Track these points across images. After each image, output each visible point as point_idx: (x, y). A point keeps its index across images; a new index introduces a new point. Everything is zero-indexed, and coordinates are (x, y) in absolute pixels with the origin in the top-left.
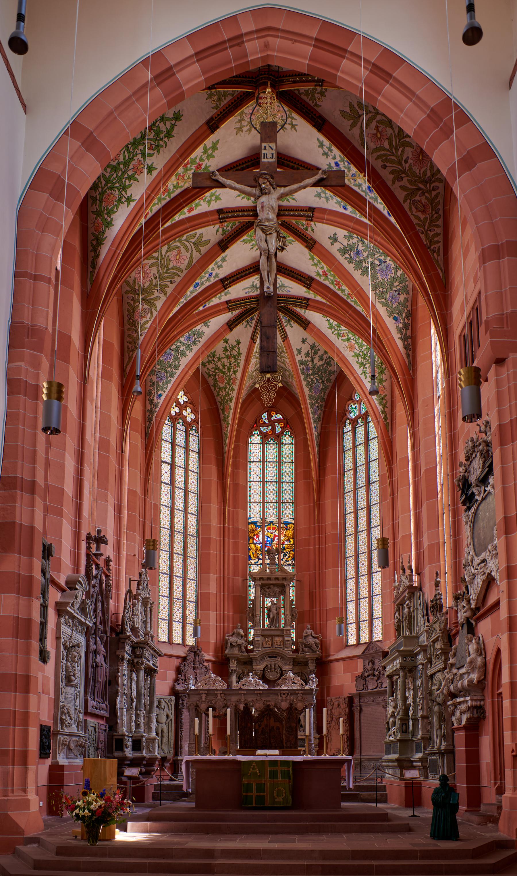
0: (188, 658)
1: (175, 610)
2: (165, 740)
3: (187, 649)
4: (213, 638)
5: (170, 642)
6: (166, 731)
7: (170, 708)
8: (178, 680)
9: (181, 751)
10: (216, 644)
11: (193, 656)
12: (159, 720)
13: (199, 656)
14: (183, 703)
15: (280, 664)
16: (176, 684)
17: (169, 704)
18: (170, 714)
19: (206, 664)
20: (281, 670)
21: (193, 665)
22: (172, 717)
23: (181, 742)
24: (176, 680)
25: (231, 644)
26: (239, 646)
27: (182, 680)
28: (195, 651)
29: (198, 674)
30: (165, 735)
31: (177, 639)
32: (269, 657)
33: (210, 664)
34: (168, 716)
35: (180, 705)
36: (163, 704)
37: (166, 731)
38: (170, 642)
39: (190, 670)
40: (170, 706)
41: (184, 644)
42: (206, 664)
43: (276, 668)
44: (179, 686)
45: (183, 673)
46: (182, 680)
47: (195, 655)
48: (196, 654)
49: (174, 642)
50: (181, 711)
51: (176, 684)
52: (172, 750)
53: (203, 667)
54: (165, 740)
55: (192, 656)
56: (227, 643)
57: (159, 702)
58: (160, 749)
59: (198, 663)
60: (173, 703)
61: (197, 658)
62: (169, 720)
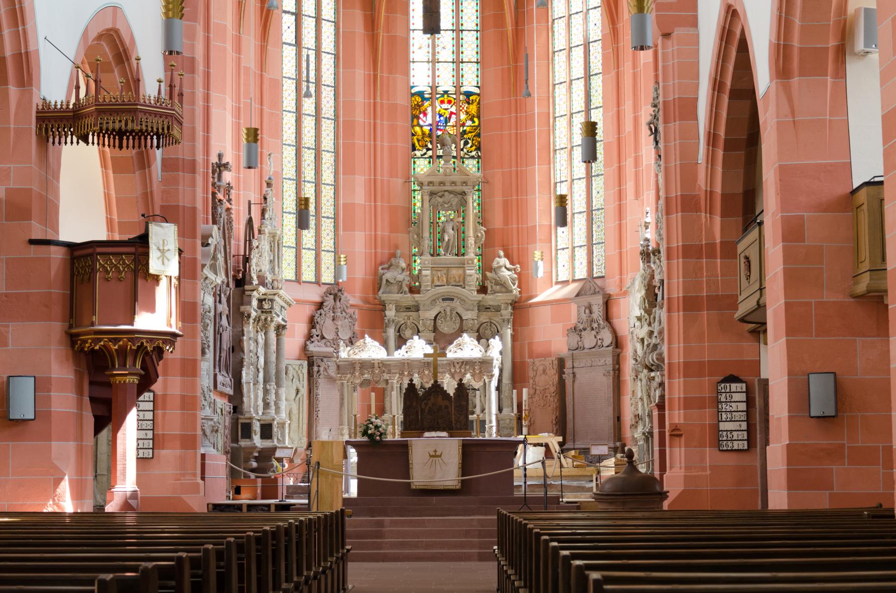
0: (325, 304)
3: (324, 288)
5: (298, 280)
6: (295, 411)
7: (301, 379)
8: (312, 337)
13: (340, 300)
14: (318, 371)
16: (308, 343)
17: (299, 372)
18: (301, 388)
19: (351, 311)
20: (461, 317)
21: (333, 314)
22: (304, 391)
23: (316, 427)
24: (309, 337)
25: (387, 281)
26: (400, 284)
27: (317, 336)
28: (335, 292)
29: (339, 327)
31: (308, 275)
32: (443, 300)
33: (357, 311)
34: (298, 391)
35: (315, 374)
36: (291, 372)
37: (295, 411)
38: (298, 280)
39: (329, 322)
40: (301, 375)
41: (318, 282)
42: (351, 311)
43: (453, 315)
45: (318, 326)
46: (317, 336)
47: (335, 300)
51: (308, 343)
56: (381, 279)
59: (339, 310)
60: (305, 371)
62: (299, 395)
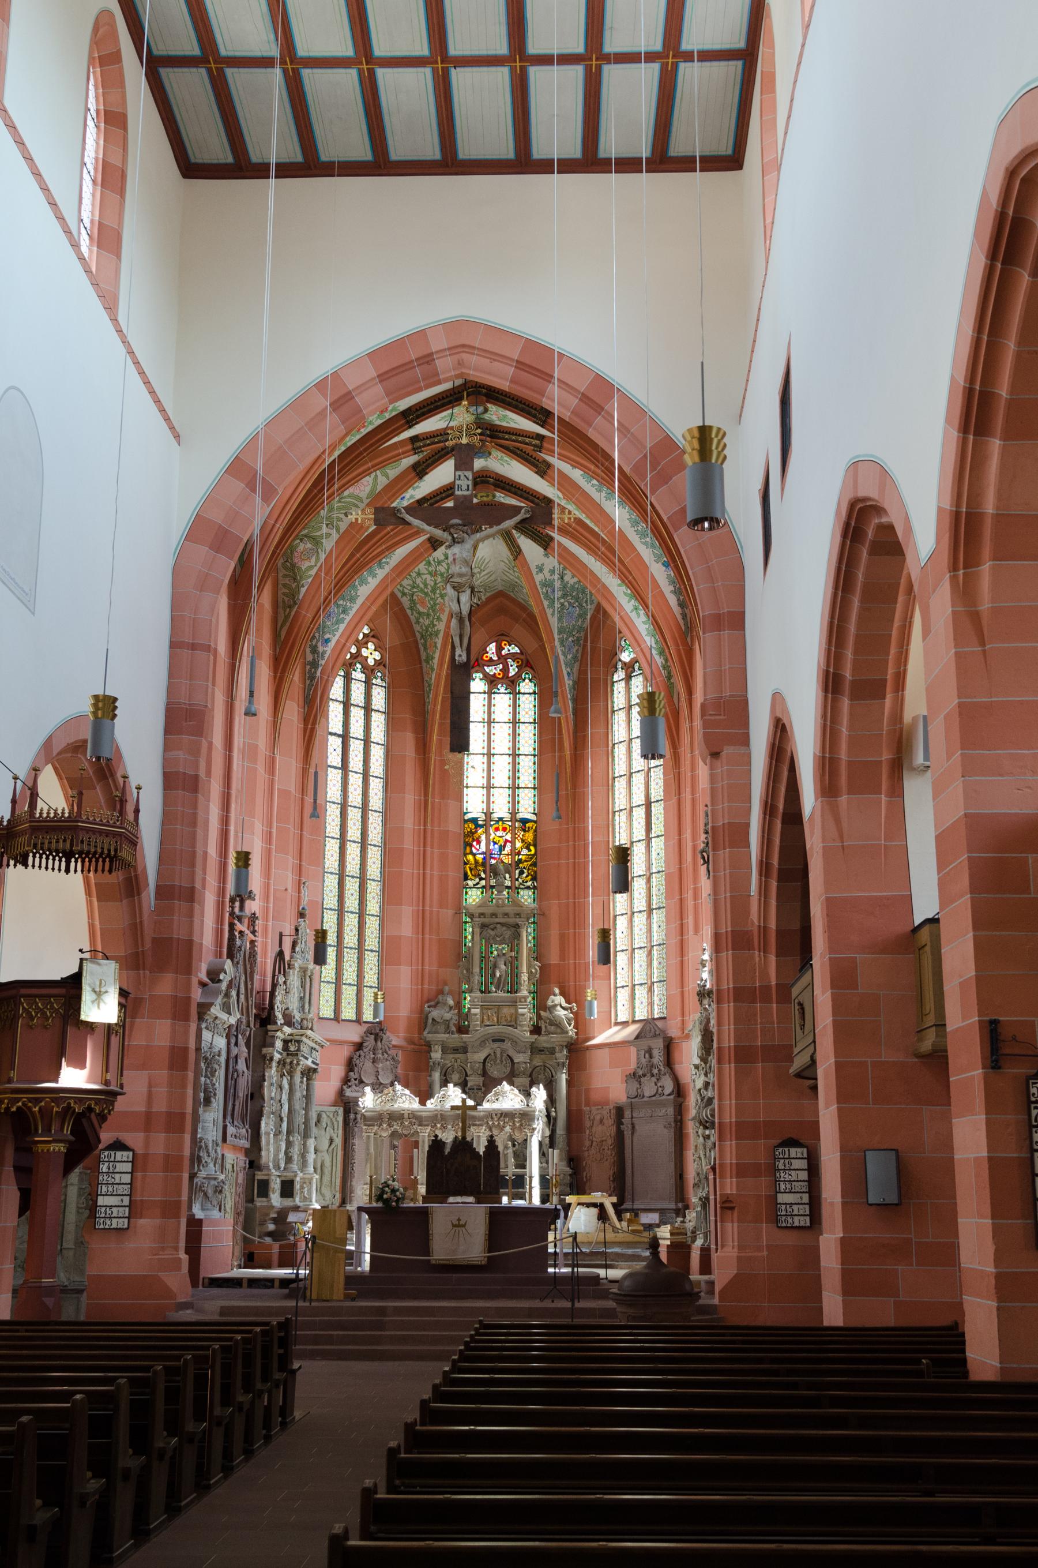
0: (365, 1044)
1: (346, 965)
2: (327, 1178)
3: (365, 1027)
4: (405, 1009)
5: (337, 1018)
6: (328, 1163)
7: (336, 1127)
8: (349, 1081)
9: (350, 1197)
10: (409, 1018)
11: (373, 1041)
12: (320, 1148)
13: (381, 1040)
14: (355, 1119)
15: (511, 1053)
16: (345, 1087)
17: (334, 1119)
18: (335, 1137)
19: (392, 1052)
20: (512, 1060)
21: (372, 1056)
22: (339, 1141)
23: (351, 1181)
24: (346, 1081)
25: (433, 1020)
26: (447, 1023)
27: (355, 1080)
28: (376, 1031)
29: (380, 1070)
30: (327, 1171)
31: (348, 1012)
32: (494, 1041)
33: (400, 1053)
34: (331, 1141)
35: (351, 1121)
36: (325, 1119)
37: (328, 1163)
38: (337, 1018)
39: (368, 1064)
40: (335, 1123)
41: (358, 1021)
42: (392, 1052)
43: (504, 1058)
44: (349, 1090)
45: (356, 1069)
46: (355, 1080)
47: (376, 1040)
48: (377, 1038)
49: (343, 1018)
50: (353, 1130)
51: (345, 1087)
52: (338, 1196)
53: (389, 1058)
54: (327, 1178)
55: (370, 1041)
56: (427, 1018)
57: (319, 1116)
58: (318, 1193)
59: (380, 1052)
60: (340, 1119)
61: (379, 1043)
62: (333, 1146)
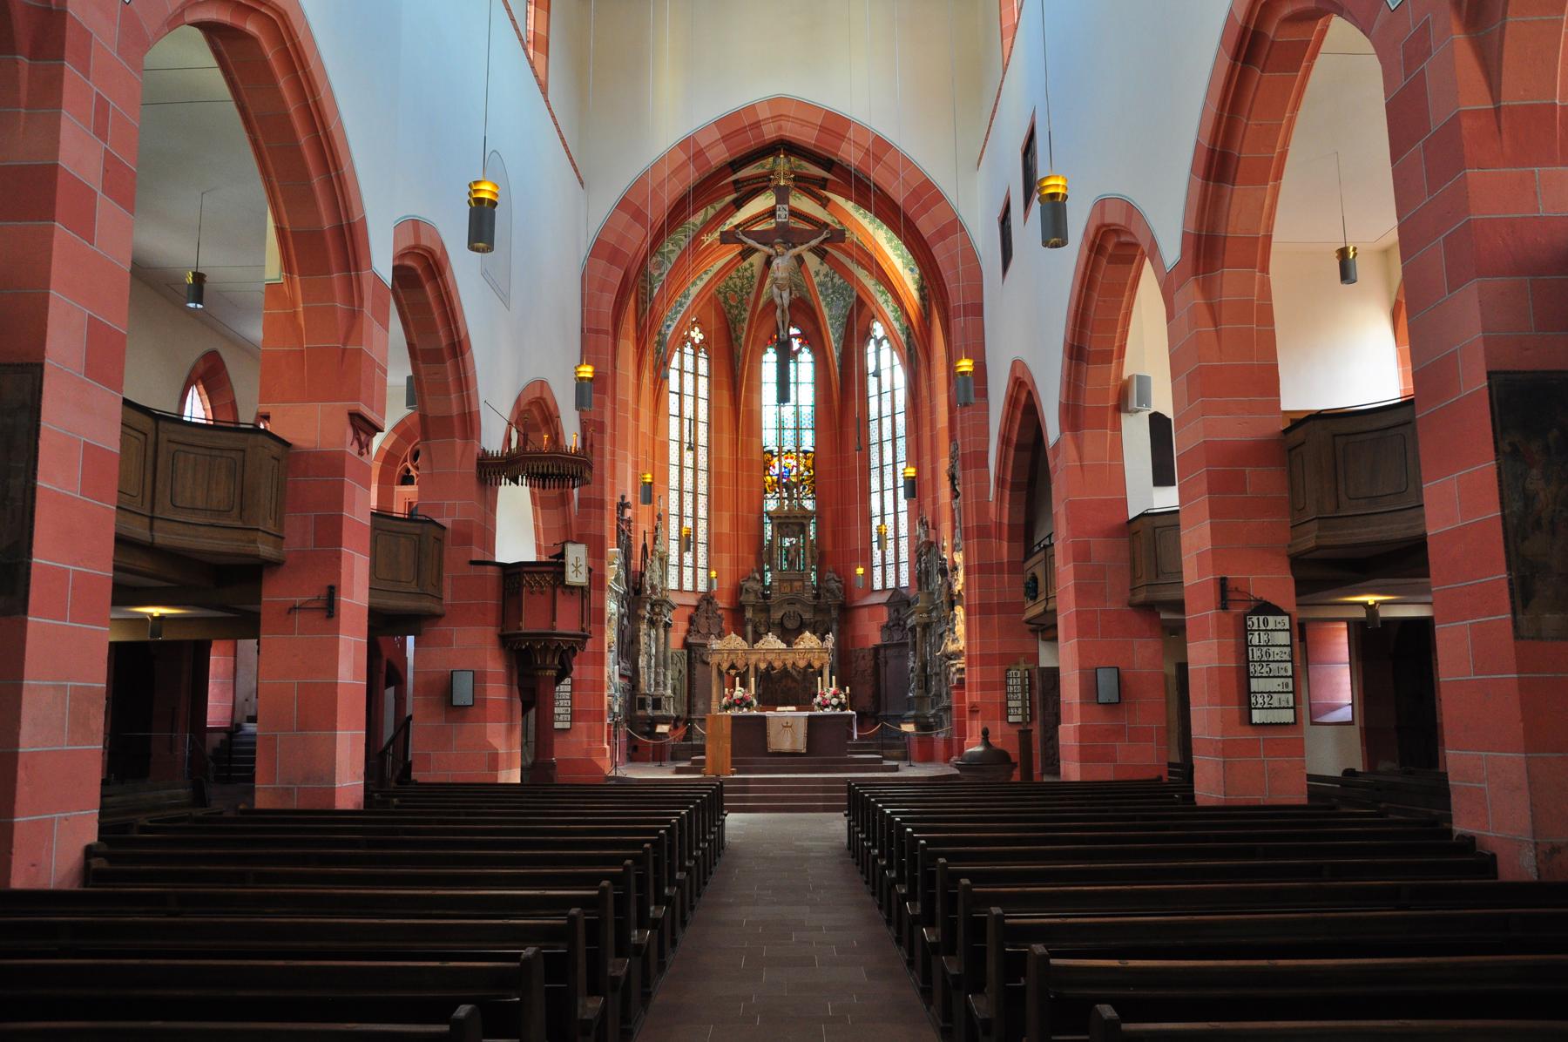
5: (680, 589)
6: (678, 687)
15: (801, 612)
19: (719, 612)
20: (802, 619)
22: (685, 672)
24: (689, 632)
25: (746, 590)
26: (756, 592)
28: (707, 598)
31: (688, 586)
34: (680, 671)
36: (676, 658)
38: (680, 589)
39: (703, 620)
41: (695, 591)
47: (708, 603)
52: (686, 708)
56: (742, 589)
60: (686, 658)
